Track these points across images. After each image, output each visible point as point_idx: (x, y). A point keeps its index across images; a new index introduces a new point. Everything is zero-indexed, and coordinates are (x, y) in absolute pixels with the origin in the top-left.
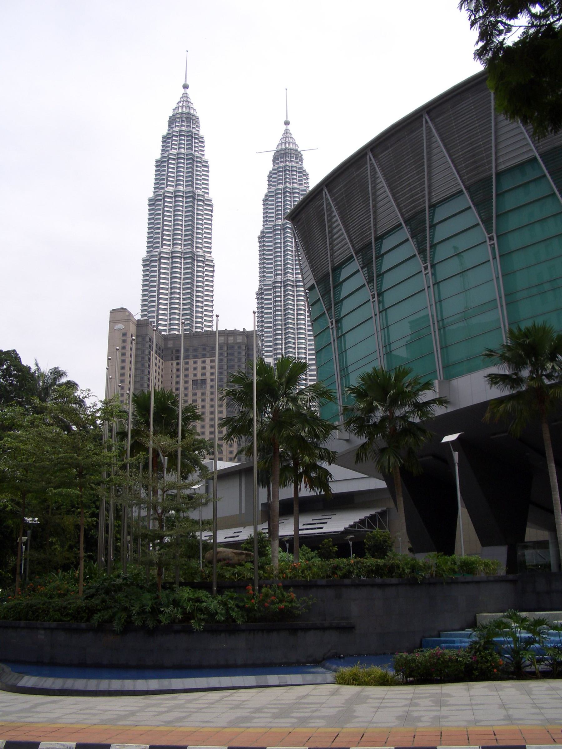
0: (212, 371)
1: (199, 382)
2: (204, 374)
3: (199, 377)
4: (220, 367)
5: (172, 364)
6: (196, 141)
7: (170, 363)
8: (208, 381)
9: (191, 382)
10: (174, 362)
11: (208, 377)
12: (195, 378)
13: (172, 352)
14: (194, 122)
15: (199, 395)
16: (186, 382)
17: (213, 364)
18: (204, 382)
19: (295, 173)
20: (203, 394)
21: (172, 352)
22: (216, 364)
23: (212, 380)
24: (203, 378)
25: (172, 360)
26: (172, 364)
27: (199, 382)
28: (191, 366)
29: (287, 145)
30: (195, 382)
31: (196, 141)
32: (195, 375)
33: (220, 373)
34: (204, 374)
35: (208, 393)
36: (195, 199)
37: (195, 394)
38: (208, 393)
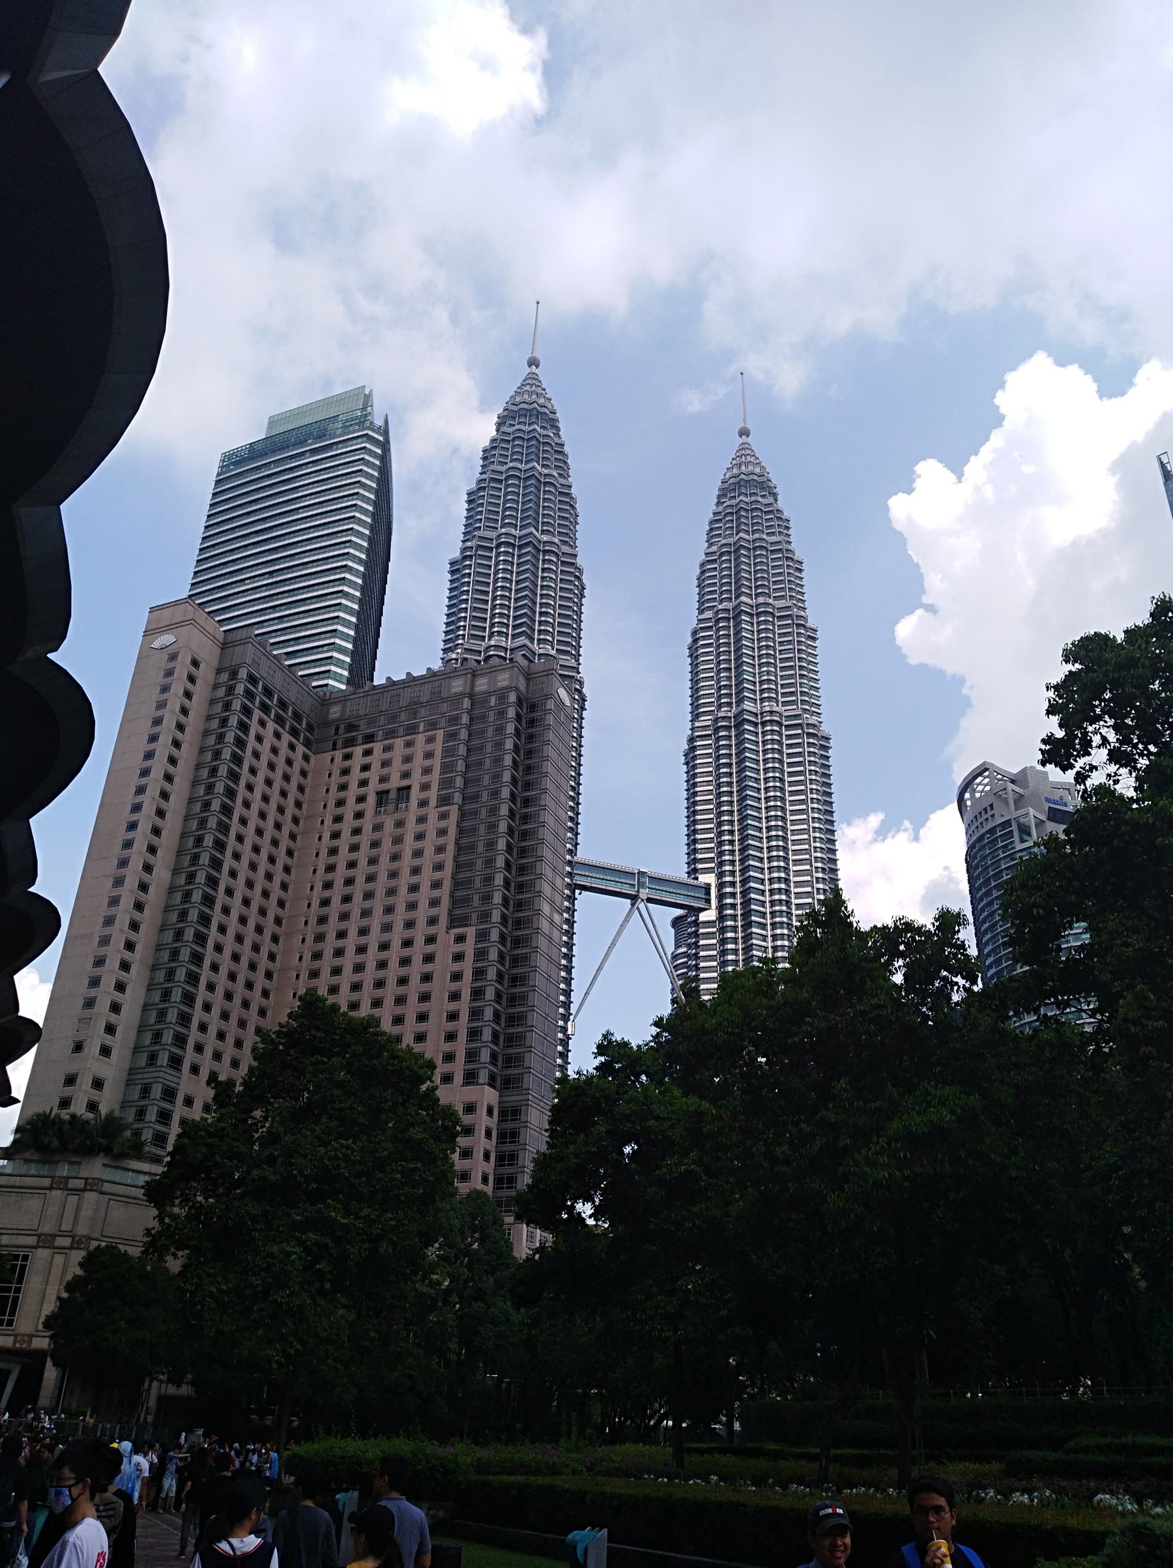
0: (428, 763)
1: (393, 795)
3: (395, 782)
5: (332, 760)
7: (328, 756)
9: (372, 799)
10: (338, 755)
11: (416, 780)
12: (384, 787)
13: (337, 729)
17: (430, 747)
20: (400, 824)
21: (337, 729)
22: (438, 747)
23: (425, 787)
24: (405, 783)
25: (334, 749)
26: (332, 760)
27: (393, 795)
29: (743, 468)
30: (382, 796)
33: (447, 768)
34: (406, 775)
37: (377, 828)
38: (412, 819)
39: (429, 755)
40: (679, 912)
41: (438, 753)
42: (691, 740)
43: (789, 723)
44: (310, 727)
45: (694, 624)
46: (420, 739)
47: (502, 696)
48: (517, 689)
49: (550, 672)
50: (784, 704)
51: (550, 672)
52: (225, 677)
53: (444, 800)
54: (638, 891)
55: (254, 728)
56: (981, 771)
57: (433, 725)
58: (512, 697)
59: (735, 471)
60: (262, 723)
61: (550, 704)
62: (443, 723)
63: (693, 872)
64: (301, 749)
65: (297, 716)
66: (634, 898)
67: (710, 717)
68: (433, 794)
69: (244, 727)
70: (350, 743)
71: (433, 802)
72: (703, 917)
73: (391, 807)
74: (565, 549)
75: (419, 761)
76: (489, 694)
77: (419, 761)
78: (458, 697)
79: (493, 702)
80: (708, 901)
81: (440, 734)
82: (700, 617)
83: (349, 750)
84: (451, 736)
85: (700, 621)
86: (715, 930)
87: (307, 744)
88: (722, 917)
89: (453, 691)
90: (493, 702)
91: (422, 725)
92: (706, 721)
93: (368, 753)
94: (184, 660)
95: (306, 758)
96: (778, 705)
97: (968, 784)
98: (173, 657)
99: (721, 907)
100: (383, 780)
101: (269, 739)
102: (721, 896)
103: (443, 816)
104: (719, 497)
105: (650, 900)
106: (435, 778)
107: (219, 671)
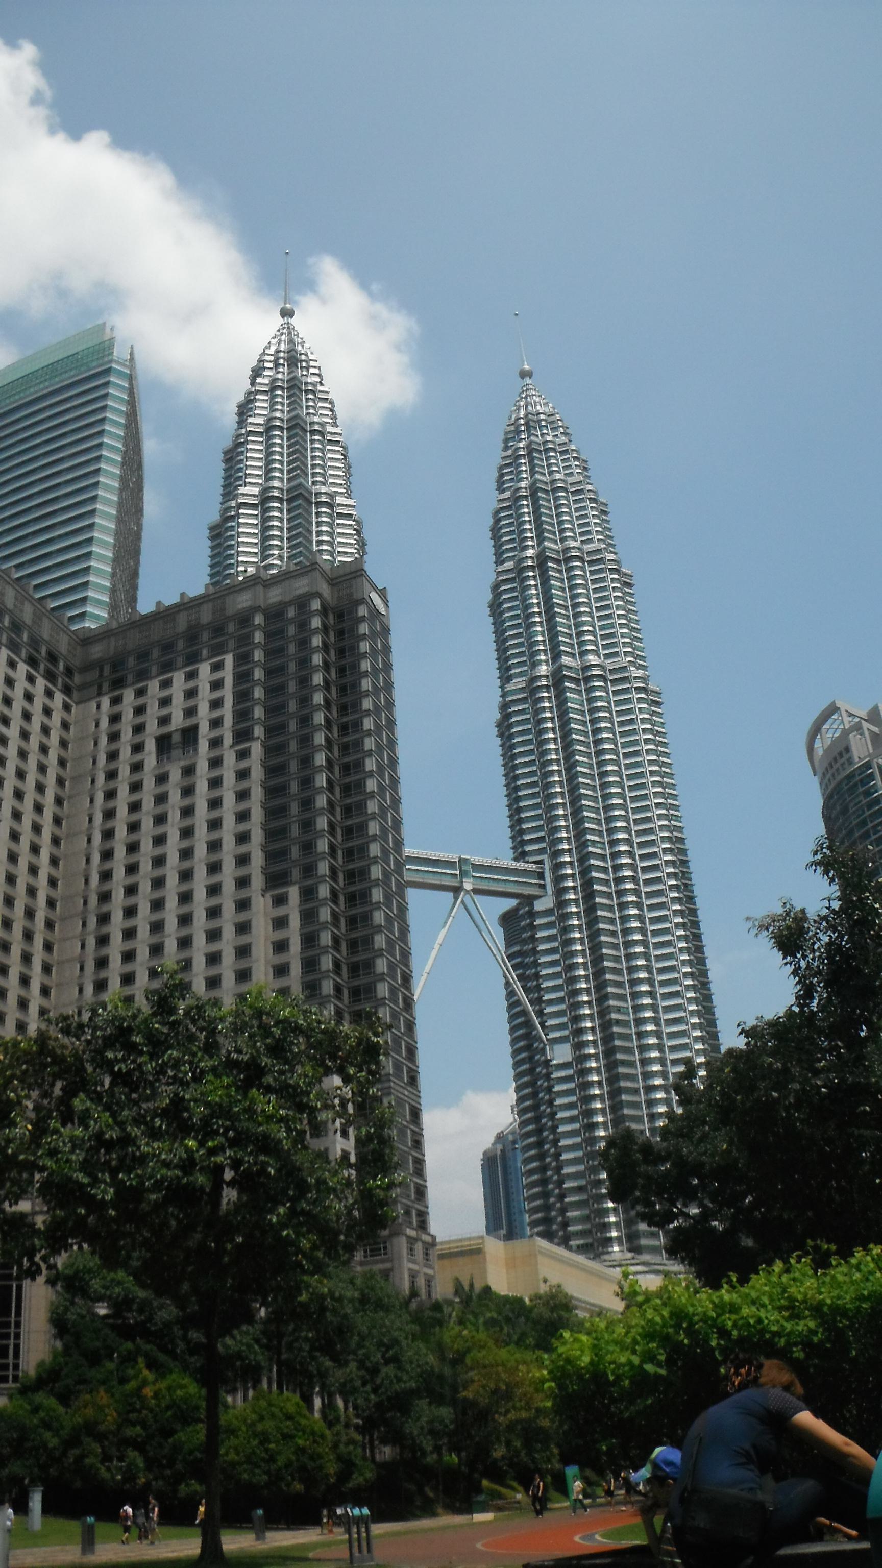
1: (177, 738)
2: (190, 712)
3: (178, 721)
4: (242, 677)
5: (98, 707)
6: (310, 396)
8: (204, 728)
9: (151, 746)
10: (106, 702)
12: (165, 730)
13: (101, 670)
14: (304, 364)
15: (175, 775)
16: (138, 748)
18: (190, 735)
19: (552, 454)
20: (189, 771)
22: (228, 674)
23: (216, 723)
24: (189, 722)
25: (100, 694)
27: (177, 738)
28: (153, 697)
29: (530, 408)
30: (164, 744)
31: (310, 396)
32: (164, 721)
33: (242, 696)
34: (190, 712)
35: (202, 766)
36: (311, 503)
37: (162, 779)
38: (202, 766)
39: (217, 685)
40: (512, 903)
42: (504, 707)
43: (615, 677)
44: (69, 672)
45: (491, 578)
46: (204, 669)
47: (302, 603)
48: (319, 595)
49: (359, 573)
50: (607, 656)
51: (359, 573)
53: (243, 735)
54: (462, 882)
57: (218, 650)
58: (316, 605)
61: (362, 611)
62: (232, 644)
63: (521, 856)
64: (59, 697)
65: (52, 658)
66: (457, 890)
67: (524, 679)
71: (228, 740)
72: (539, 906)
73: (176, 753)
75: (205, 693)
77: (205, 693)
79: (291, 613)
80: (543, 887)
81: (229, 660)
82: (500, 569)
83: (116, 693)
84: (243, 659)
85: (499, 573)
86: (553, 918)
87: (67, 690)
89: (240, 607)
90: (291, 613)
91: (205, 652)
92: (518, 683)
95: (67, 707)
96: (599, 657)
99: (560, 891)
100: (164, 721)
103: (243, 755)
104: (506, 441)
105: (476, 891)
106: (227, 711)
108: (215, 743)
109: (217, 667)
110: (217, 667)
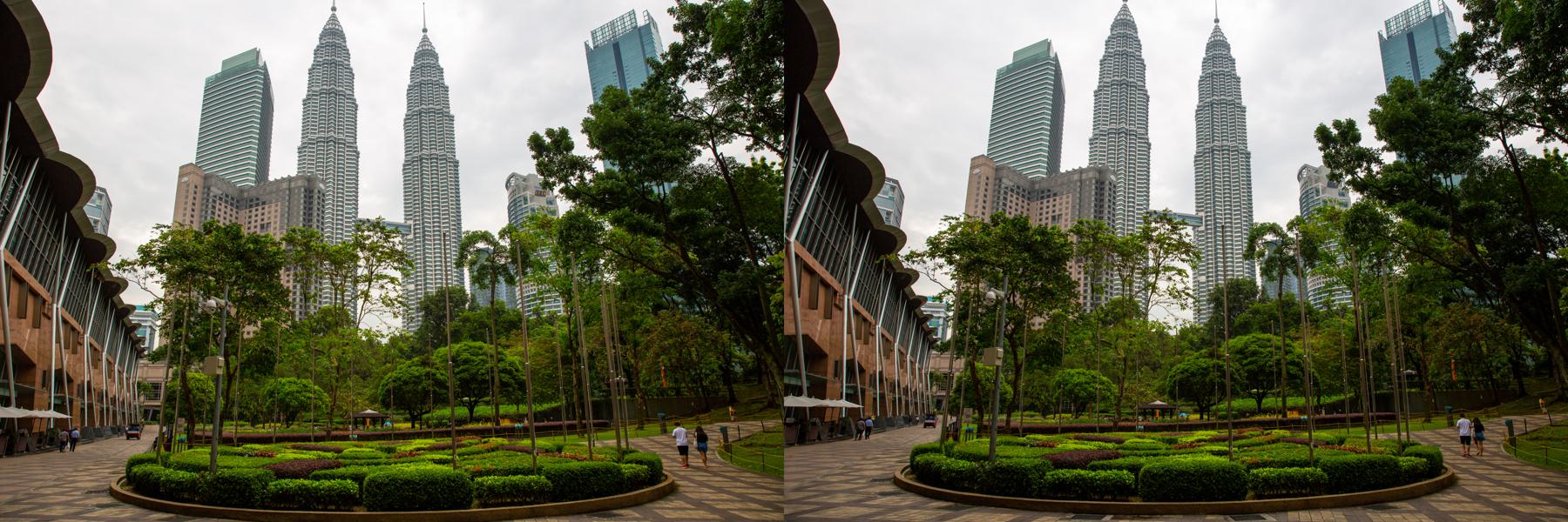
3: (266, 221)
10: (247, 211)
22: (279, 208)
33: (282, 216)
39: (276, 211)
41: (279, 210)
44: (237, 201)
52: (206, 190)
55: (218, 206)
56: (513, 175)
59: (421, 49)
60: (220, 204)
64: (235, 210)
65: (232, 199)
68: (278, 226)
69: (214, 207)
70: (251, 206)
74: (348, 92)
76: (295, 188)
78: (284, 190)
81: (279, 204)
88: (415, 238)
93: (257, 210)
94: (192, 189)
95: (237, 213)
97: (508, 181)
98: (188, 185)
100: (262, 220)
101: (223, 209)
102: (415, 229)
107: (204, 188)
108: (275, 229)
109: (277, 206)
110: (277, 206)
